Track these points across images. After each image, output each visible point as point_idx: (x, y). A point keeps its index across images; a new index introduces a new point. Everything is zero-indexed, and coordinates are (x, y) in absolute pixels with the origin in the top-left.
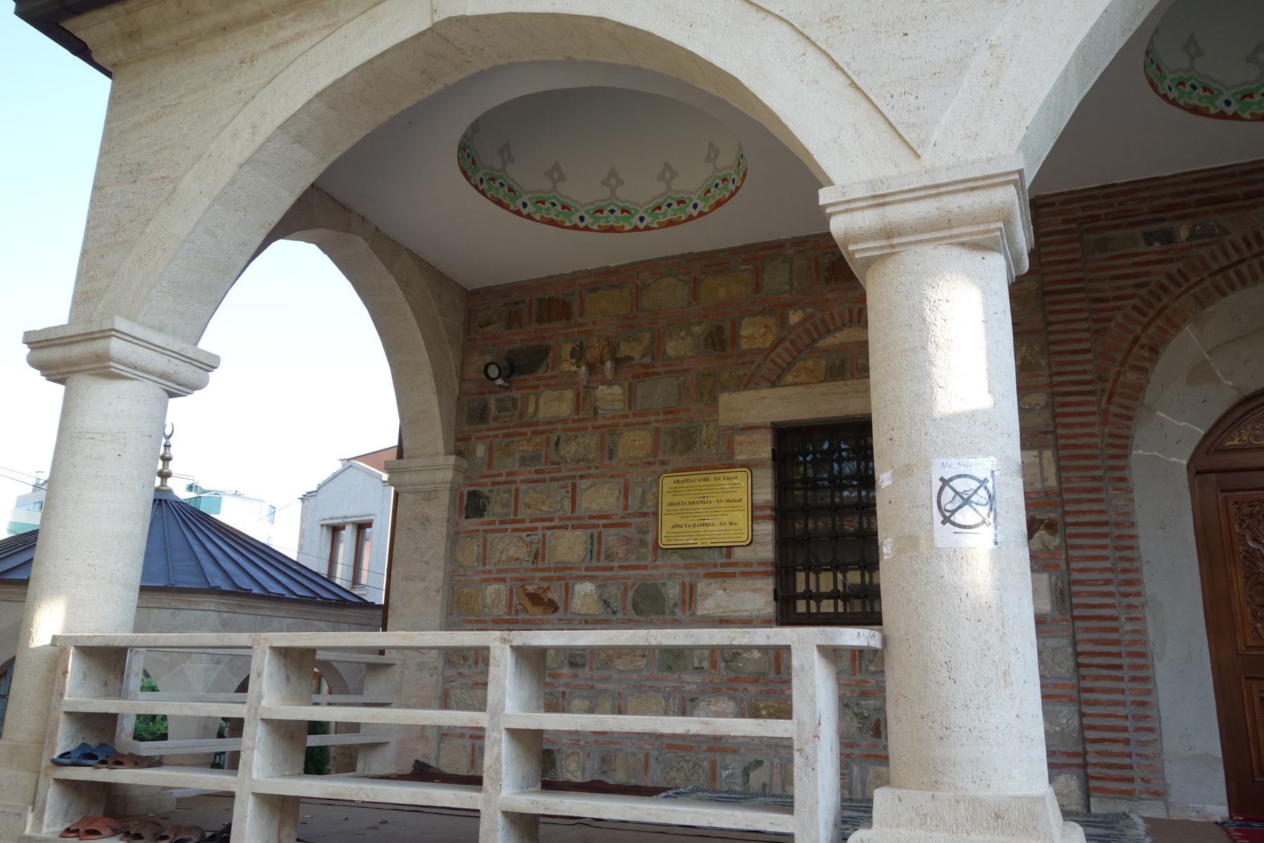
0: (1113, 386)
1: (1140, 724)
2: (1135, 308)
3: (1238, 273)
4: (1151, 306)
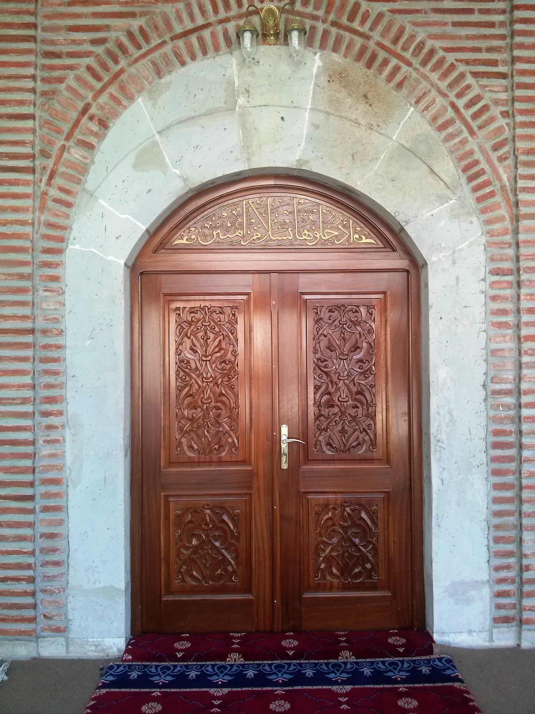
0: (55, 164)
1: (48, 558)
2: (89, 68)
3: (201, 40)
4: (105, 67)
